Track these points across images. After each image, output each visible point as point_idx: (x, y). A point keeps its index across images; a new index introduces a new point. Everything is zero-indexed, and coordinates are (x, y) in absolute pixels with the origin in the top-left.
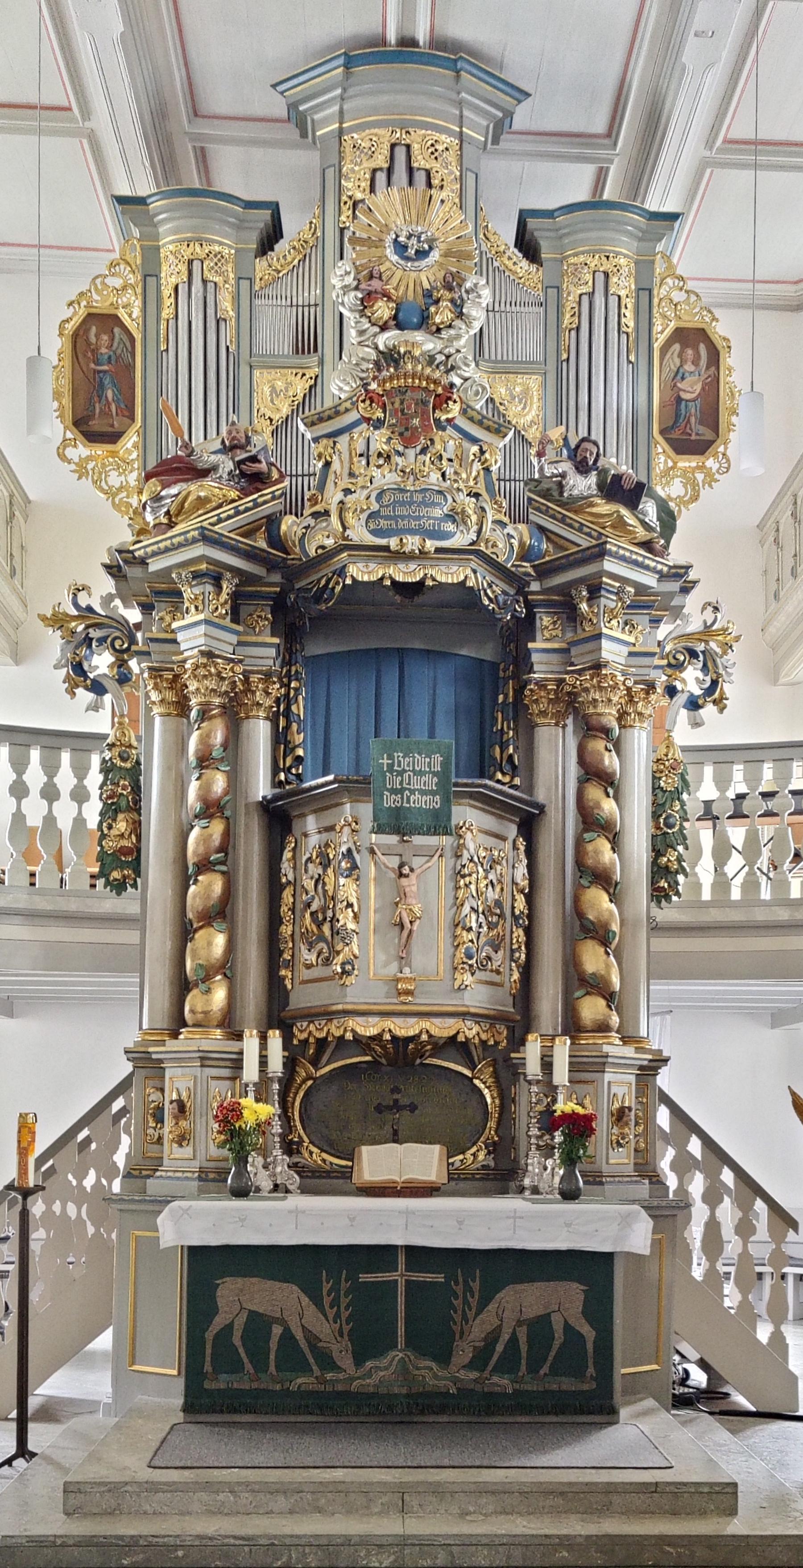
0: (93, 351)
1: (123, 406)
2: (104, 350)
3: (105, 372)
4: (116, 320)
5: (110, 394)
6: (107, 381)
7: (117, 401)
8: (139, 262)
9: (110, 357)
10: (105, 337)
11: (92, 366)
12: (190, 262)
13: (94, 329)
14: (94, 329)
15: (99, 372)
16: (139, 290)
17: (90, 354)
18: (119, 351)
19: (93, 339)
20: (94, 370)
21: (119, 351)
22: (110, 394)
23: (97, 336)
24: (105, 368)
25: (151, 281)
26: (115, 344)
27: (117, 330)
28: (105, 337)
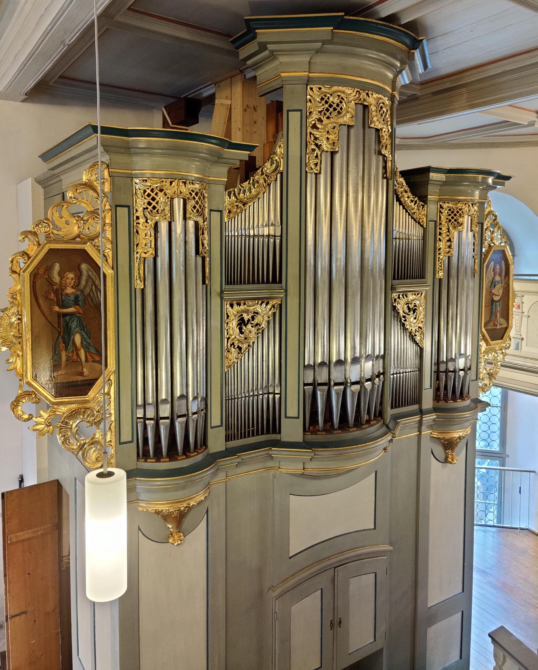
0: (56, 292)
1: (93, 350)
2: (69, 290)
3: (71, 314)
4: (84, 255)
5: (78, 339)
6: (74, 325)
7: (86, 348)
8: (107, 188)
9: (77, 297)
10: (71, 275)
11: (57, 309)
12: (172, 199)
13: (57, 267)
14: (57, 267)
15: (65, 315)
16: (108, 221)
17: (52, 296)
18: (88, 290)
19: (56, 279)
20: (59, 314)
21: (88, 290)
22: (78, 339)
23: (61, 274)
24: (71, 310)
25: (122, 212)
26: (83, 282)
27: (84, 267)
28: (71, 275)
